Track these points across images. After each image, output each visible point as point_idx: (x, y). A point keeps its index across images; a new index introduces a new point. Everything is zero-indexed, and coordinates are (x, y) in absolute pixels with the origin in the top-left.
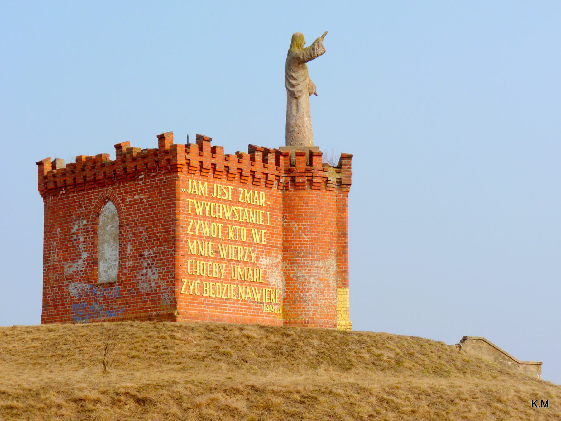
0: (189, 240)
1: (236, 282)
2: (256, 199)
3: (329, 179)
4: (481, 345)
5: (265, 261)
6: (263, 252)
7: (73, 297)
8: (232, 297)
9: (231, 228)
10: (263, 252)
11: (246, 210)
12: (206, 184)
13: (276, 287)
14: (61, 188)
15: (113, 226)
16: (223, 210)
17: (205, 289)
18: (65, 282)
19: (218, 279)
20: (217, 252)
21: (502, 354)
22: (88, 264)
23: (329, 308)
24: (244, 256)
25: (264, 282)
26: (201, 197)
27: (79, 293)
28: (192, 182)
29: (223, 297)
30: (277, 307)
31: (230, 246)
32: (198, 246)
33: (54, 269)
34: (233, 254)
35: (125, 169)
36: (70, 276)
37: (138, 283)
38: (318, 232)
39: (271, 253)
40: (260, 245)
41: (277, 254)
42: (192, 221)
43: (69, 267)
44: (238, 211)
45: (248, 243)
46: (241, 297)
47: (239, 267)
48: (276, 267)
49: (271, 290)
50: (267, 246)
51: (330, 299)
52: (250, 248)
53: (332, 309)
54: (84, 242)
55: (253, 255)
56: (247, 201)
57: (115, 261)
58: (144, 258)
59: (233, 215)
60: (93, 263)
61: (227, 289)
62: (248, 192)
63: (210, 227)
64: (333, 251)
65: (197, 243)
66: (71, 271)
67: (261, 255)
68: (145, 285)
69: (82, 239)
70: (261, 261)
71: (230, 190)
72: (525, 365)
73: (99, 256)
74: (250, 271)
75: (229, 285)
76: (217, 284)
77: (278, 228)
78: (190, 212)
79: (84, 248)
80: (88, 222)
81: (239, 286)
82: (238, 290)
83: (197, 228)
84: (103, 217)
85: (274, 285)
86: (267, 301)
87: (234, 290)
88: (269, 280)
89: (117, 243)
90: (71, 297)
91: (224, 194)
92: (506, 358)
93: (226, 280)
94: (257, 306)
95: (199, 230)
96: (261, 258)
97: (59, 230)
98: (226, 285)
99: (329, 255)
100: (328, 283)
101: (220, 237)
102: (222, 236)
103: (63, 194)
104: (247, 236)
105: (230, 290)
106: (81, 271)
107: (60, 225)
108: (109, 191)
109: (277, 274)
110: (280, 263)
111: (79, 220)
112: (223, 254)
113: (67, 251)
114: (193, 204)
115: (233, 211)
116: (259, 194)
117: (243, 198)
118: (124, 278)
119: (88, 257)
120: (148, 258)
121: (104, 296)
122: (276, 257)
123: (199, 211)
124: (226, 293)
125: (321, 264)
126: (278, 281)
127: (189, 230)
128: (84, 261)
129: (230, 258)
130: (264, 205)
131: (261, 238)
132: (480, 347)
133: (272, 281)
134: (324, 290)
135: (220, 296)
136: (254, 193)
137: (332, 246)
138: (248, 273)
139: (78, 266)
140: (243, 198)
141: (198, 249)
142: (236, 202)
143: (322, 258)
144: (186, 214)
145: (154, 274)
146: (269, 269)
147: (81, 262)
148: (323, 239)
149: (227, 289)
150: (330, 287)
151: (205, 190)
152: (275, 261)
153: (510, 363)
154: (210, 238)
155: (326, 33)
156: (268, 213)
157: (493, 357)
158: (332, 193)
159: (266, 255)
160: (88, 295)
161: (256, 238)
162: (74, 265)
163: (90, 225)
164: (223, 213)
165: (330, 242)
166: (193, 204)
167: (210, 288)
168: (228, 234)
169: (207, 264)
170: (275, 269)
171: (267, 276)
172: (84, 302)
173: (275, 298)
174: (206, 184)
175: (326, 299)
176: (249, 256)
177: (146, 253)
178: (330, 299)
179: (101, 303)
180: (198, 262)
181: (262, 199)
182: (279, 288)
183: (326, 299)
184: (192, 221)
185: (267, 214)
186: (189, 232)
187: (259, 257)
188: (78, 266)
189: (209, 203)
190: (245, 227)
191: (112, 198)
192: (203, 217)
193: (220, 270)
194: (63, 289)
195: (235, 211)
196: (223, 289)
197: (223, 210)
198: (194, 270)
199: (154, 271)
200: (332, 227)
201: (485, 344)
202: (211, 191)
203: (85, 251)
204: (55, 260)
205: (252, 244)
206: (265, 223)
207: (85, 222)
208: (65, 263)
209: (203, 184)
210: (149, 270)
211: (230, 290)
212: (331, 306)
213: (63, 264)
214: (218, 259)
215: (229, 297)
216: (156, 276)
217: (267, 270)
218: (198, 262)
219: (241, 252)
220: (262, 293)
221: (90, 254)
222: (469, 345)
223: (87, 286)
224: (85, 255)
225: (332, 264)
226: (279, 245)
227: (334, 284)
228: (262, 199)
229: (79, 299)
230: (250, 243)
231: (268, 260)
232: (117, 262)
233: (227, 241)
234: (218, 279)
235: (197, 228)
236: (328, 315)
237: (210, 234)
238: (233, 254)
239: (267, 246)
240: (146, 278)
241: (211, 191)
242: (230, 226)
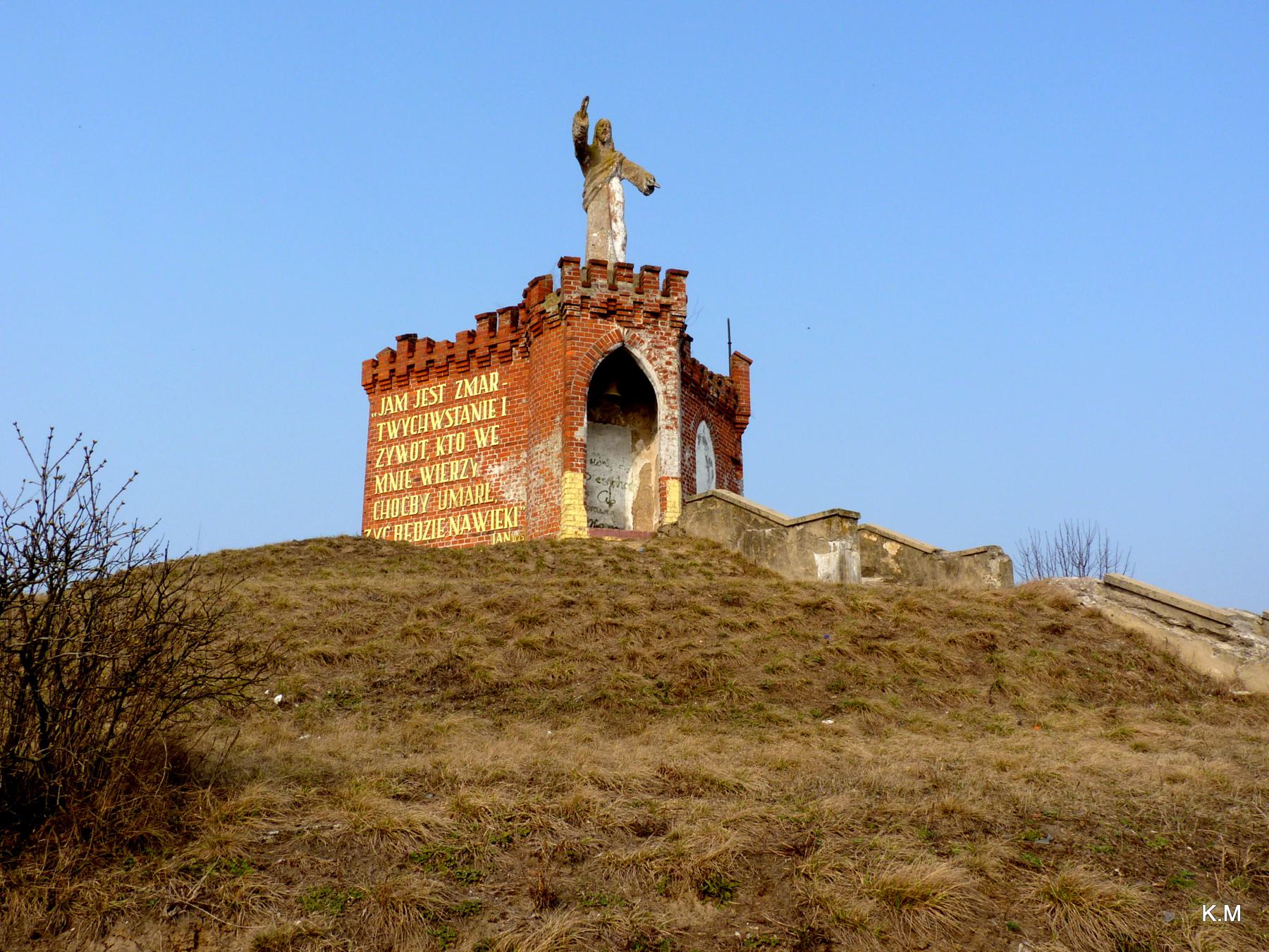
0: (377, 477)
1: (447, 513)
2: (483, 386)
3: (547, 311)
4: (712, 508)
5: (496, 470)
6: (495, 456)
8: (439, 536)
9: (441, 439)
10: (495, 456)
11: (466, 407)
12: (406, 396)
13: (517, 502)
16: (429, 420)
17: (396, 534)
19: (417, 516)
20: (419, 479)
21: (752, 515)
23: (551, 515)
24: (459, 474)
25: (492, 500)
26: (398, 415)
28: (386, 400)
29: (425, 539)
30: (517, 533)
31: (438, 466)
32: (389, 480)
34: (443, 475)
38: (540, 399)
39: (509, 454)
40: (489, 448)
41: (520, 452)
42: (383, 450)
44: (452, 413)
45: (468, 453)
46: (454, 533)
47: (451, 491)
48: (517, 472)
49: (506, 510)
50: (503, 446)
51: (553, 498)
52: (471, 459)
53: (556, 514)
55: (475, 469)
56: (468, 394)
59: (446, 421)
61: (431, 527)
62: (470, 382)
63: (409, 451)
64: (558, 419)
65: (389, 476)
67: (490, 462)
70: (491, 471)
71: (441, 390)
72: (801, 527)
74: (469, 491)
75: (434, 521)
76: (416, 524)
77: (523, 414)
78: (380, 439)
81: (451, 518)
82: (449, 525)
83: (389, 457)
85: (512, 501)
86: (498, 527)
87: (442, 526)
88: (503, 495)
91: (433, 398)
92: (761, 521)
93: (430, 514)
94: (480, 539)
95: (393, 458)
96: (490, 466)
98: (429, 522)
99: (553, 428)
100: (550, 474)
101: (423, 457)
102: (426, 456)
104: (467, 443)
105: (436, 526)
109: (517, 483)
110: (525, 464)
112: (426, 479)
114: (385, 428)
115: (445, 416)
116: (488, 378)
117: (462, 392)
122: (518, 457)
123: (393, 433)
124: (430, 532)
125: (541, 447)
126: (520, 492)
127: (378, 461)
129: (437, 482)
130: (496, 389)
131: (489, 439)
132: (710, 513)
133: (509, 495)
134: (545, 486)
135: (419, 539)
136: (479, 379)
137: (556, 412)
138: (464, 494)
140: (462, 392)
141: (388, 485)
142: (452, 402)
143: (543, 436)
144: (376, 444)
146: (504, 479)
148: (545, 406)
149: (431, 527)
150: (552, 478)
151: (403, 405)
152: (515, 465)
153: (768, 531)
154: (407, 465)
155: (587, 99)
156: (504, 399)
157: (734, 527)
158: (559, 330)
159: (498, 461)
161: (482, 441)
164: (430, 424)
165: (554, 407)
166: (385, 428)
167: (404, 532)
168: (436, 450)
169: (401, 501)
170: (514, 476)
171: (500, 490)
173: (512, 520)
174: (406, 396)
175: (547, 500)
176: (470, 470)
178: (553, 498)
180: (388, 501)
181: (494, 381)
182: (521, 502)
183: (547, 500)
184: (383, 450)
185: (502, 401)
186: (377, 466)
187: (487, 467)
189: (409, 419)
190: (464, 431)
192: (400, 439)
193: (417, 503)
195: (449, 416)
196: (424, 528)
197: (429, 420)
198: (382, 513)
200: (558, 382)
201: (719, 505)
202: (412, 400)
205: (476, 450)
206: (498, 415)
209: (401, 397)
211: (436, 526)
212: (554, 509)
214: (421, 488)
215: (433, 537)
217: (501, 481)
218: (388, 501)
219: (455, 468)
220: (489, 518)
222: (690, 516)
225: (555, 442)
226: (523, 439)
227: (556, 472)
228: (494, 381)
230: (472, 451)
231: (502, 467)
233: (434, 460)
234: (417, 516)
235: (389, 457)
236: (549, 526)
237: (409, 459)
238: (443, 475)
239: (503, 446)
241: (412, 400)
242: (439, 439)
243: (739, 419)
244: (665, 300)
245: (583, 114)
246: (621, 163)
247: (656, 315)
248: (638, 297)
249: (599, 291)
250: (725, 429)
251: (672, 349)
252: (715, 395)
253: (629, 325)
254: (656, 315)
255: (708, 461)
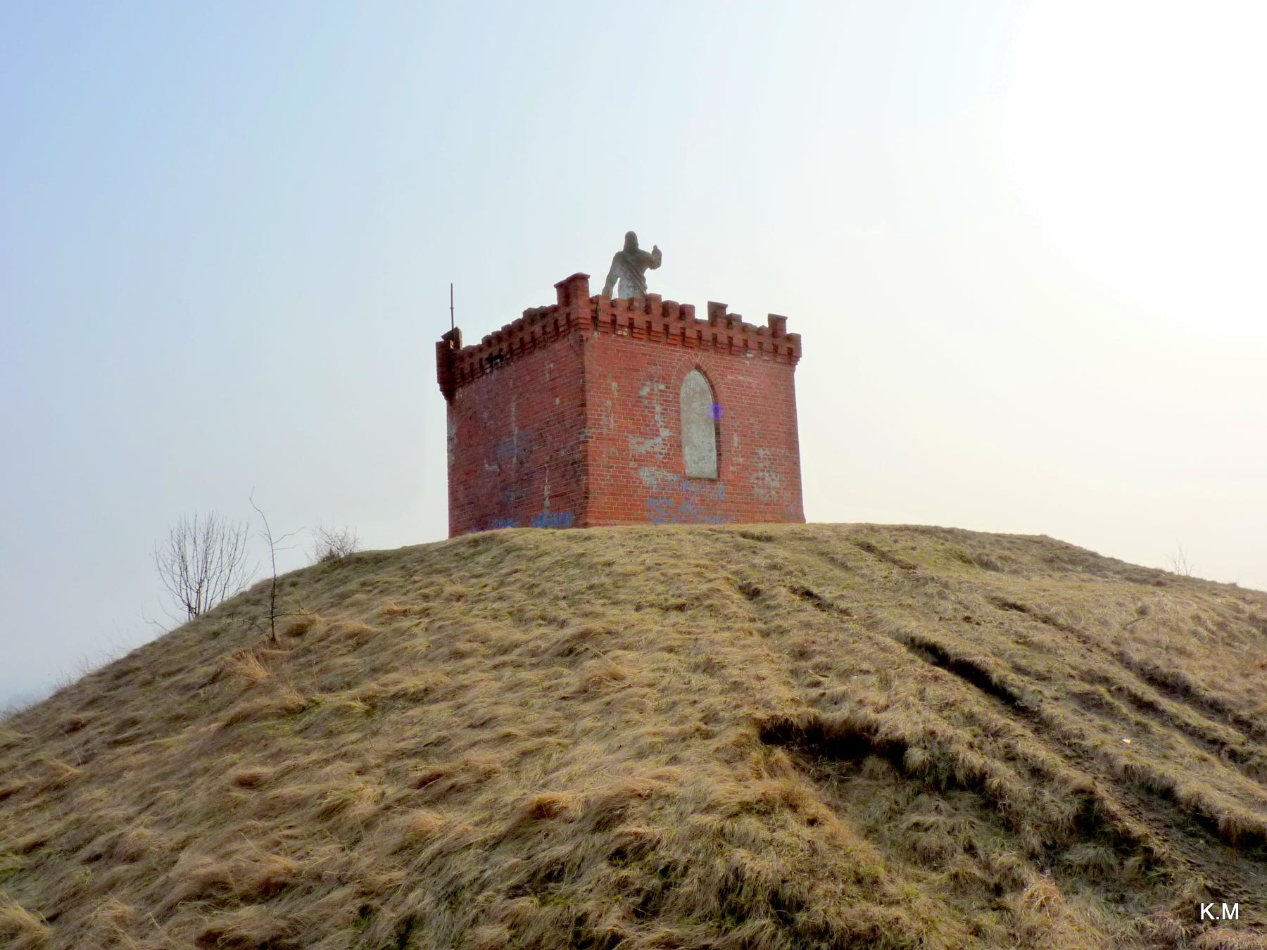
7: (649, 488)
14: (622, 326)
15: (702, 405)
18: (632, 464)
22: (672, 446)
27: (658, 484)
33: (610, 440)
35: (730, 338)
36: (640, 456)
37: (753, 487)
43: (639, 443)
54: (662, 414)
57: (710, 451)
58: (759, 458)
60: (676, 445)
66: (642, 449)
68: (762, 491)
69: (658, 409)
73: (684, 437)
79: (664, 422)
80: (667, 387)
84: (686, 387)
89: (711, 429)
90: (644, 487)
97: (615, 385)
103: (622, 336)
106: (661, 454)
107: (616, 378)
108: (700, 357)
111: (651, 380)
113: (631, 419)
118: (730, 477)
119: (671, 437)
120: (765, 459)
121: (702, 496)
128: (664, 440)
139: (656, 445)
145: (773, 480)
147: (658, 440)
160: (676, 490)
162: (647, 442)
163: (671, 393)
172: (668, 498)
177: (761, 452)
179: (696, 504)
188: (656, 445)
191: (704, 368)
194: (628, 473)
199: (774, 477)
203: (665, 427)
204: (612, 426)
207: (662, 387)
208: (631, 436)
210: (767, 474)
213: (628, 437)
216: (776, 484)
221: (674, 433)
223: (670, 477)
224: (665, 433)
229: (660, 493)
232: (714, 454)
240: (763, 483)
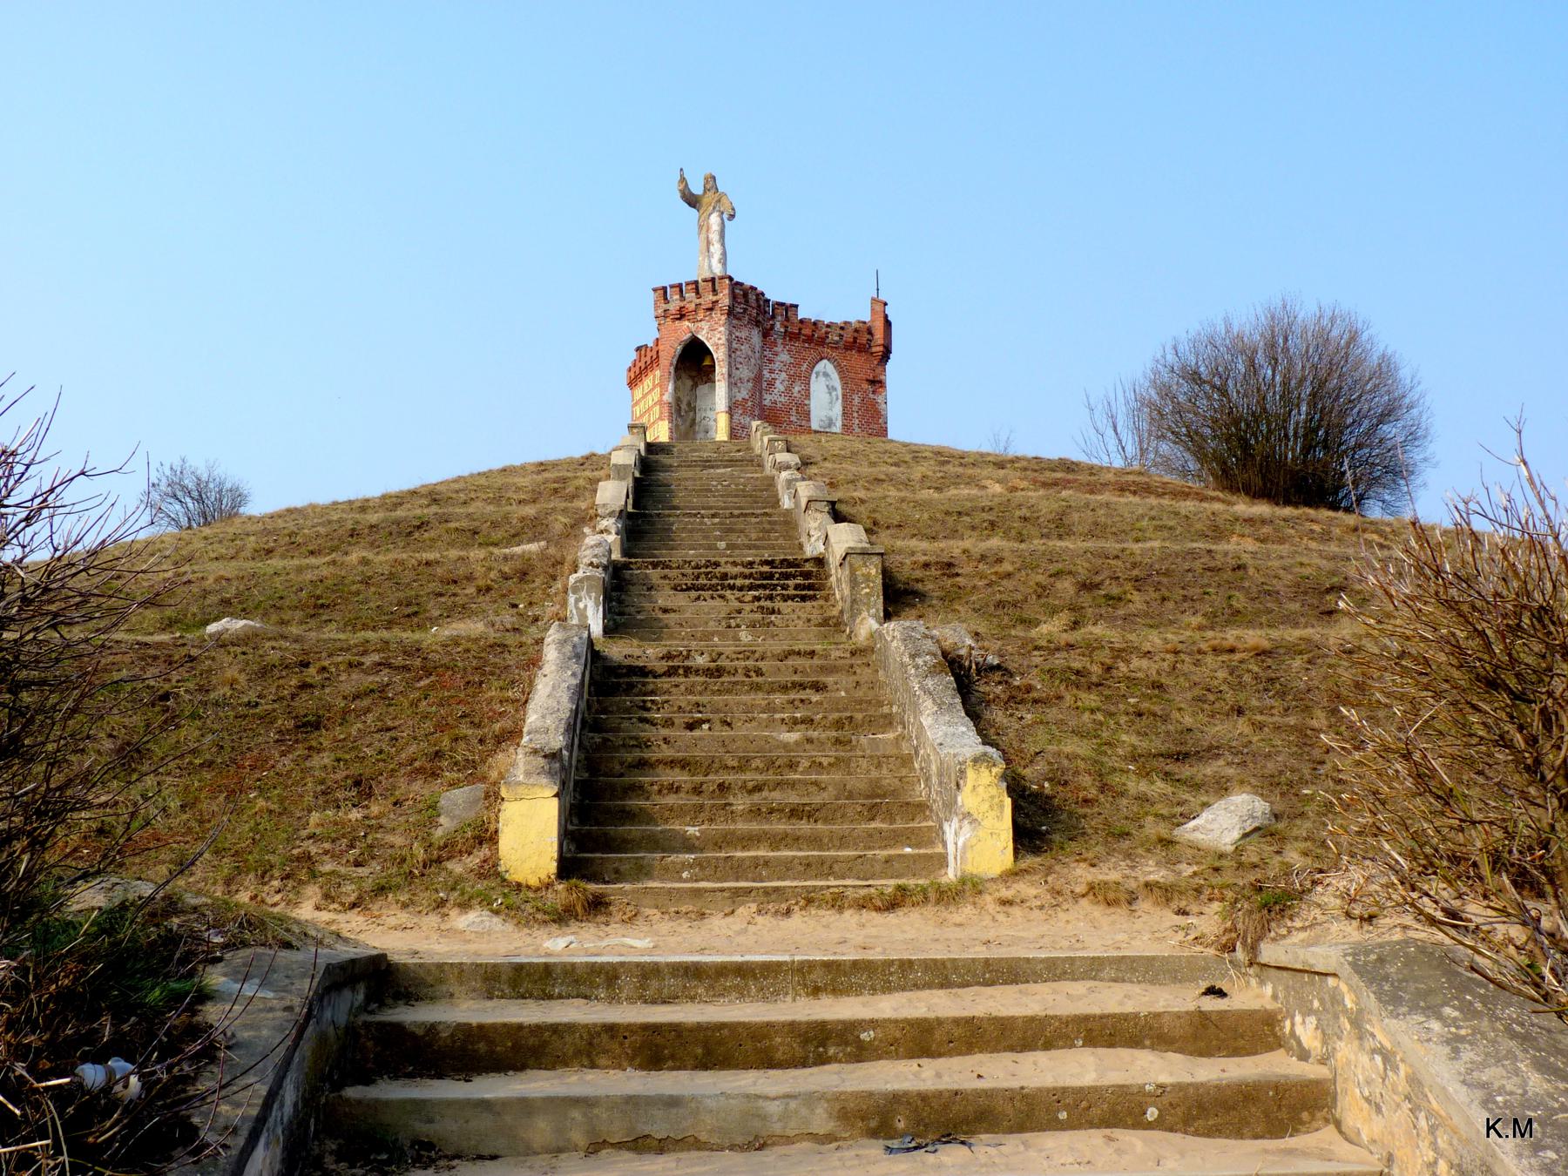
243: (874, 350)
244: (715, 298)
245: (683, 179)
246: (719, 201)
247: (711, 309)
248: (698, 301)
249: (675, 304)
250: (855, 359)
251: (722, 329)
252: (837, 338)
253: (695, 321)
254: (711, 309)
255: (831, 389)
